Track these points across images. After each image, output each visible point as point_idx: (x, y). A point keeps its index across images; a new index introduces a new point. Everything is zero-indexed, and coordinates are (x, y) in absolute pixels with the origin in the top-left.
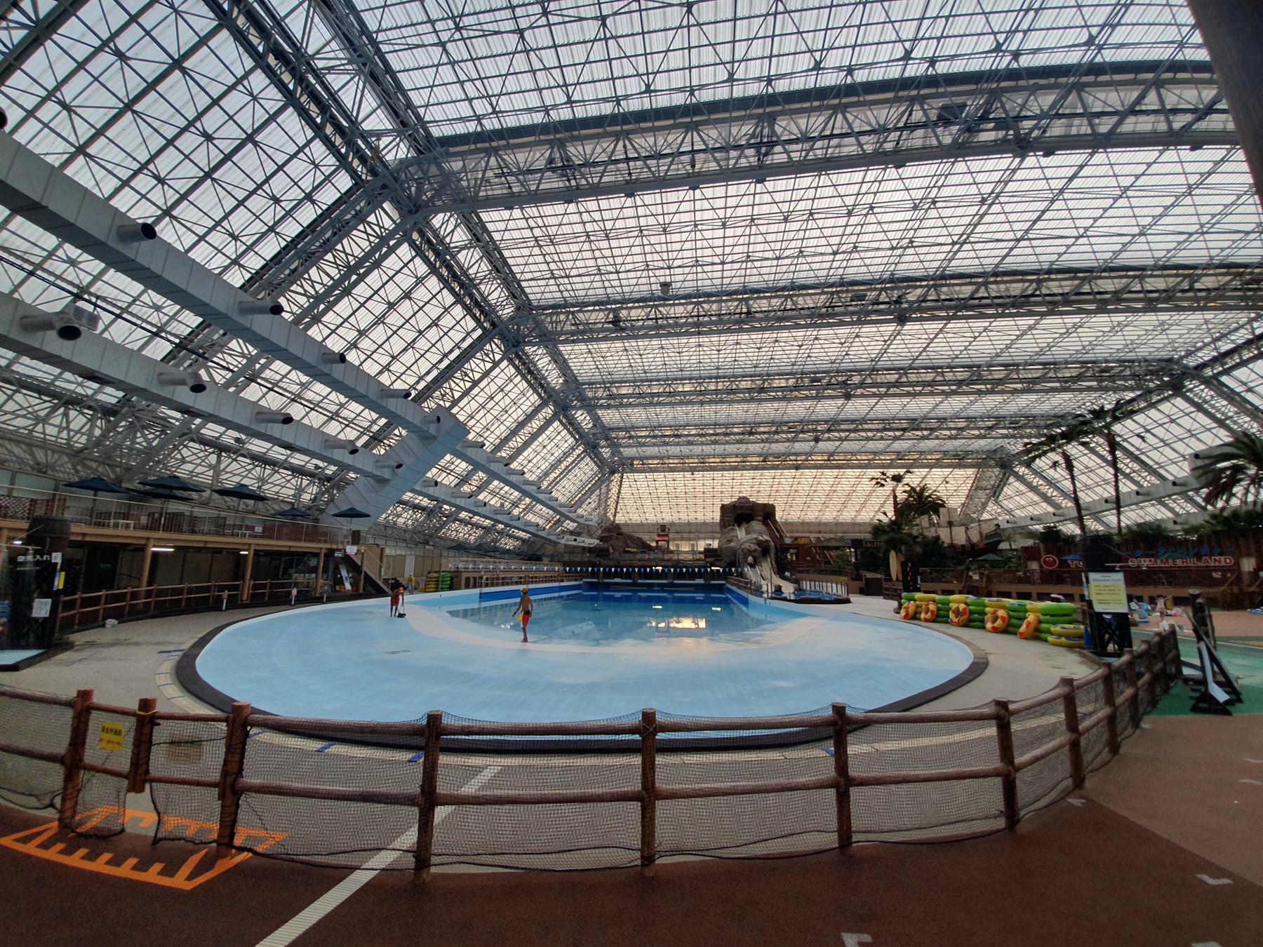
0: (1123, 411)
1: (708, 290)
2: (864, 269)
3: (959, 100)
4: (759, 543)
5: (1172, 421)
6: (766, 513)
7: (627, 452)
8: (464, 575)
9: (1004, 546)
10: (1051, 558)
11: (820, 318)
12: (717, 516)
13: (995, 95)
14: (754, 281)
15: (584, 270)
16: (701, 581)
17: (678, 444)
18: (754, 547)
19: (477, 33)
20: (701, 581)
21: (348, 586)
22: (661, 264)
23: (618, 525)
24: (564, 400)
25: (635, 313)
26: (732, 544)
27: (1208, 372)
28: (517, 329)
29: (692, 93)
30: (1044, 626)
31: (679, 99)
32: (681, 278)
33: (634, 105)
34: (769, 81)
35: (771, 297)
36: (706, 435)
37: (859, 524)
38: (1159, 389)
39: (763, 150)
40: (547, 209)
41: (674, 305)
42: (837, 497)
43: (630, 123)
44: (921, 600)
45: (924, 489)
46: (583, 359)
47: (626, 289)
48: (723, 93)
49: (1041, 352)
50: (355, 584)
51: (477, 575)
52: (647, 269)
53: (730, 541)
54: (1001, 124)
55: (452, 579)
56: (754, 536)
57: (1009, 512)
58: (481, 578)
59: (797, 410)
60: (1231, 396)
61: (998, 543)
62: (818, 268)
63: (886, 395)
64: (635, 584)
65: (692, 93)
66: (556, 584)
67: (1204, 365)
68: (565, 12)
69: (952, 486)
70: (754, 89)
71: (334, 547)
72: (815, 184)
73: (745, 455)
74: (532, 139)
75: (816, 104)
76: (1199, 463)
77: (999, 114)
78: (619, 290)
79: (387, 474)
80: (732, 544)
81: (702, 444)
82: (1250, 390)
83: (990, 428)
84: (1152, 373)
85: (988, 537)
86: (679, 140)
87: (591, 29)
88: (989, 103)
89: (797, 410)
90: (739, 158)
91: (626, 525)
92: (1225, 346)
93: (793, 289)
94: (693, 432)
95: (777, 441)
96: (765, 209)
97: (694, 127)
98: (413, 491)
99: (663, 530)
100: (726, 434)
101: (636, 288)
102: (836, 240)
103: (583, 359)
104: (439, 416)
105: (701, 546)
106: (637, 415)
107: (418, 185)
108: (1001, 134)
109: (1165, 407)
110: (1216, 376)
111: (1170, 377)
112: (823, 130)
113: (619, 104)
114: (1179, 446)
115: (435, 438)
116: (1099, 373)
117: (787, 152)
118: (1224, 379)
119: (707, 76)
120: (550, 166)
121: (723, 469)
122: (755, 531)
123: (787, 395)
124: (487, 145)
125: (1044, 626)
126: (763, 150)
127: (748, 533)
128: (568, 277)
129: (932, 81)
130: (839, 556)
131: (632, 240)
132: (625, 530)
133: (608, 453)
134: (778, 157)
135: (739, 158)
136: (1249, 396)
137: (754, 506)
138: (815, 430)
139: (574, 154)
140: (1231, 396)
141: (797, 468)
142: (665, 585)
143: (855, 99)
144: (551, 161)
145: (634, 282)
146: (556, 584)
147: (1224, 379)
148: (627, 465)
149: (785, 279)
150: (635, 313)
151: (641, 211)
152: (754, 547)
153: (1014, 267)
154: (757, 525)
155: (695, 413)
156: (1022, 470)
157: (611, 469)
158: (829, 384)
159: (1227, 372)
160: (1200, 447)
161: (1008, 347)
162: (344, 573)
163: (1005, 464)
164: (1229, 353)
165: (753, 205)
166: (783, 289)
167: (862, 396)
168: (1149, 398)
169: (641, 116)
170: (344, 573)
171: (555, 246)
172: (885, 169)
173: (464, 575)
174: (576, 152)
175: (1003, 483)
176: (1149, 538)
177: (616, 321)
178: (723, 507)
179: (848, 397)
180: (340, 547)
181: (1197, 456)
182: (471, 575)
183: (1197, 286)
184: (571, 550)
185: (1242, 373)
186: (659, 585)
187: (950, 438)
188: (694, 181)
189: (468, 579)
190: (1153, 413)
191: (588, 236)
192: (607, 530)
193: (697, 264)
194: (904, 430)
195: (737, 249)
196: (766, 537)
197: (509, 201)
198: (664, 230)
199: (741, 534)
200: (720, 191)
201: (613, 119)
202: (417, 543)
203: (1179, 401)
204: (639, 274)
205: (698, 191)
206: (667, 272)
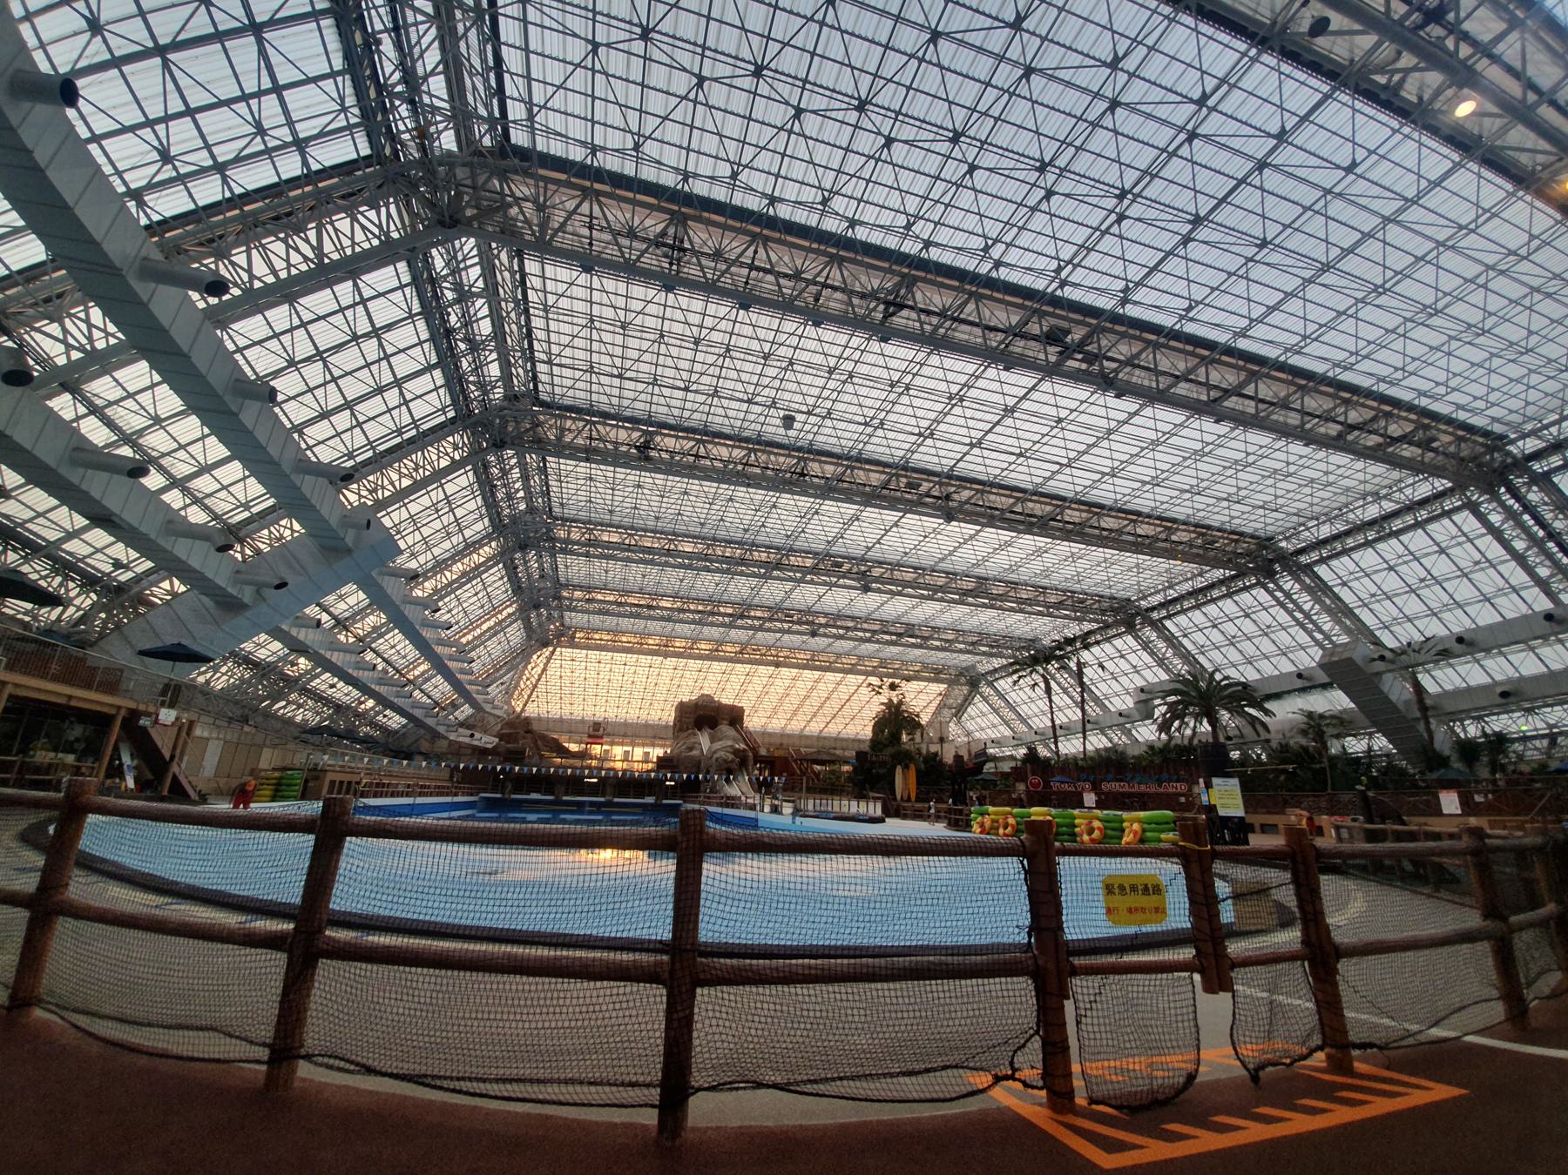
0: (1085, 641)
1: (663, 418)
2: (936, 460)
3: (1064, 324)
4: (736, 752)
5: (1122, 656)
6: (734, 716)
7: (573, 618)
8: (330, 777)
9: (989, 767)
10: (1037, 779)
11: (872, 497)
12: (669, 716)
13: (1095, 332)
14: (718, 422)
15: (569, 361)
16: (650, 800)
17: (587, 612)
18: (731, 757)
19: (555, 25)
20: (650, 800)
21: (131, 783)
22: (741, 396)
23: (527, 718)
24: (523, 534)
25: (670, 443)
26: (695, 753)
27: (1155, 615)
28: (504, 425)
29: (685, 180)
30: (1149, 834)
31: (669, 180)
32: (631, 395)
33: (611, 163)
34: (853, 223)
35: (733, 447)
36: (626, 604)
37: (807, 737)
38: (1117, 624)
39: (891, 309)
40: (638, 291)
41: (617, 426)
42: (830, 706)
43: (602, 182)
44: (996, 814)
45: (901, 703)
46: (578, 486)
47: (557, 390)
48: (720, 194)
49: (1011, 570)
50: (142, 784)
51: (355, 778)
52: (591, 370)
53: (691, 749)
54: (1091, 358)
55: (306, 781)
56: (730, 743)
57: (968, 734)
58: (358, 783)
59: (806, 595)
60: (1171, 640)
61: (985, 762)
62: (889, 445)
63: (900, 594)
64: (558, 802)
65: (685, 180)
66: (449, 799)
67: (1153, 609)
68: (668, 61)
69: (922, 698)
70: (753, 203)
71: (142, 707)
72: (799, 332)
73: (671, 637)
74: (563, 177)
75: (815, 246)
76: (1143, 696)
77: (1092, 348)
78: (615, 401)
79: (247, 595)
80: (695, 753)
81: (619, 615)
82: (1185, 636)
83: (973, 644)
84: (1112, 609)
85: (977, 755)
86: (739, 250)
87: (577, 50)
88: (1089, 336)
89: (806, 595)
90: (874, 309)
91: (539, 719)
92: (1172, 594)
93: (759, 443)
94: (611, 598)
95: (712, 624)
96: (743, 343)
97: (834, 260)
98: (277, 634)
99: (597, 731)
100: (649, 607)
101: (571, 393)
102: (811, 401)
103: (578, 486)
104: (366, 519)
105: (657, 752)
106: (614, 572)
107: (456, 190)
108: (1084, 366)
109: (1118, 642)
110: (1160, 620)
111: (1124, 615)
112: (818, 275)
113: (594, 154)
114: (1124, 680)
115: (349, 551)
116: (1074, 602)
117: (922, 324)
118: (1168, 623)
119: (705, 166)
120: (658, 242)
121: (691, 657)
122: (727, 738)
123: (805, 575)
124: (588, 184)
125: (1149, 834)
126: (891, 309)
127: (713, 740)
128: (620, 376)
129: (1056, 302)
130: (833, 772)
131: (576, 329)
132: (535, 727)
133: (544, 615)
134: (903, 319)
135: (874, 309)
136: (1185, 642)
137: (720, 708)
138: (813, 623)
139: (683, 234)
140: (1171, 640)
141: (777, 665)
142: (600, 804)
143: (852, 255)
144: (663, 234)
145: (569, 383)
146: (449, 799)
147: (1168, 623)
148: (565, 637)
149: (752, 429)
150: (670, 443)
151: (621, 302)
152: (731, 757)
153: (1055, 491)
154: (725, 728)
155: (672, 579)
156: (987, 690)
157: (539, 640)
158: (849, 571)
159: (1169, 617)
160: (1140, 683)
161: (985, 560)
162: (126, 759)
163: (974, 681)
164: (1175, 600)
165: (731, 334)
166: (747, 440)
167: (879, 591)
168: (1104, 633)
169: (618, 180)
170: (126, 759)
171: (594, 330)
172: (869, 340)
173: (330, 777)
174: (700, 236)
175: (967, 701)
176: (1110, 765)
177: (644, 448)
178: (681, 704)
179: (866, 589)
180: (151, 709)
181: (1142, 690)
182: (338, 777)
183: (1174, 538)
184: (457, 750)
185: (1181, 619)
186: (592, 804)
187: (913, 646)
188: (746, 300)
189: (333, 783)
190: (1107, 647)
191: (592, 321)
192: (510, 724)
193: (654, 383)
194: (874, 632)
195: (704, 379)
196: (743, 746)
197: (588, 262)
198: (662, 336)
199: (704, 740)
200: (698, 305)
201: (582, 170)
202: (231, 720)
203: (1129, 639)
204: (578, 374)
205: (671, 296)
206: (616, 382)
